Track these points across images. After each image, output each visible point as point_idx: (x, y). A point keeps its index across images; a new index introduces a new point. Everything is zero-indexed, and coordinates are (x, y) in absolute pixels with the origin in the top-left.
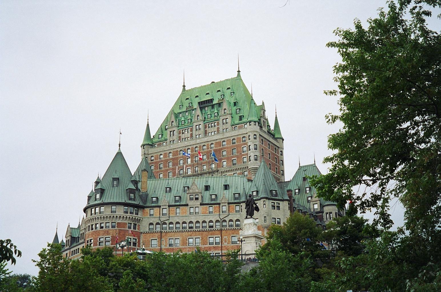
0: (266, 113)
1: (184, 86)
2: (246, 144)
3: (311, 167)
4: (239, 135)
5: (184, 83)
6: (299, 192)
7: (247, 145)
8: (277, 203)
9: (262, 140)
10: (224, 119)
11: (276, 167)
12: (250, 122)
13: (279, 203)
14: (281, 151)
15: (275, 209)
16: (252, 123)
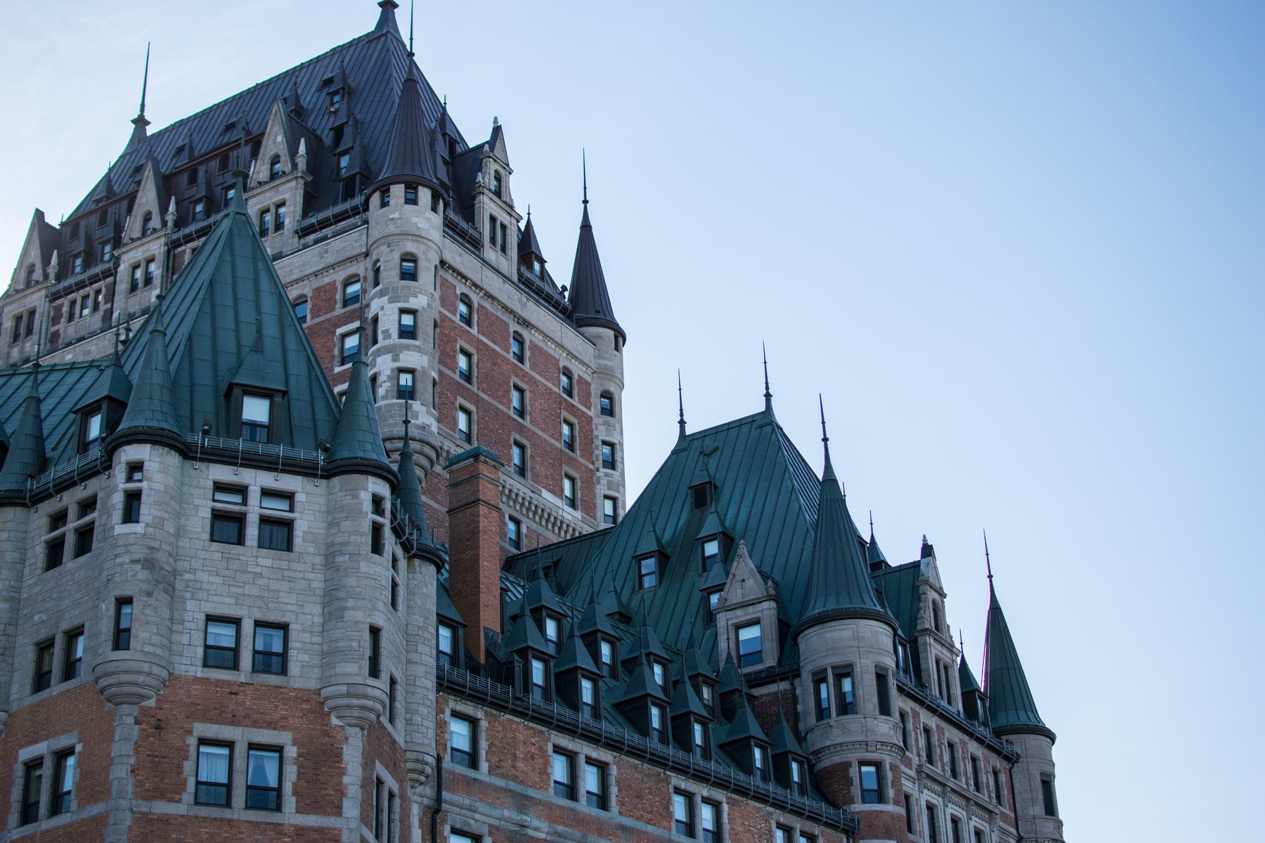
0: (512, 185)
1: (141, 122)
2: (360, 314)
3: (745, 429)
4: (326, 269)
5: (142, 110)
6: (662, 572)
7: (364, 320)
8: (266, 493)
9: (466, 300)
10: (267, 211)
11: (566, 468)
12: (385, 192)
13: (289, 496)
14: (607, 395)
15: (240, 541)
16: (398, 191)
